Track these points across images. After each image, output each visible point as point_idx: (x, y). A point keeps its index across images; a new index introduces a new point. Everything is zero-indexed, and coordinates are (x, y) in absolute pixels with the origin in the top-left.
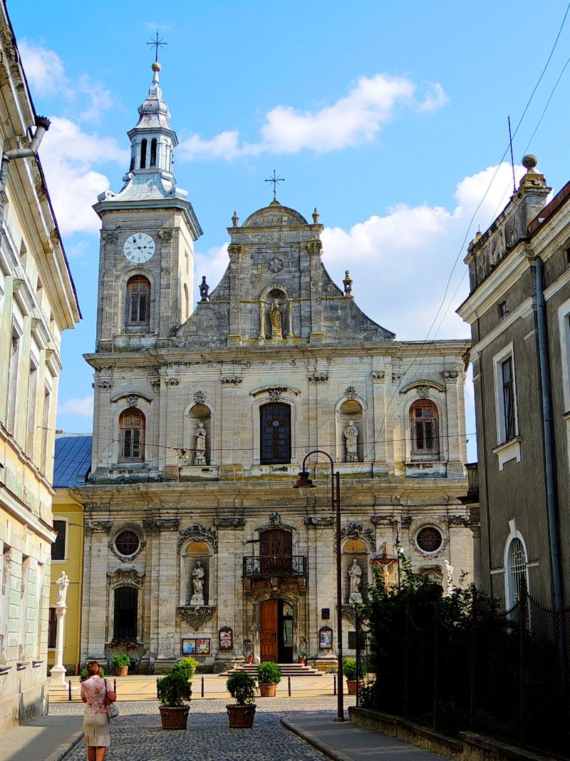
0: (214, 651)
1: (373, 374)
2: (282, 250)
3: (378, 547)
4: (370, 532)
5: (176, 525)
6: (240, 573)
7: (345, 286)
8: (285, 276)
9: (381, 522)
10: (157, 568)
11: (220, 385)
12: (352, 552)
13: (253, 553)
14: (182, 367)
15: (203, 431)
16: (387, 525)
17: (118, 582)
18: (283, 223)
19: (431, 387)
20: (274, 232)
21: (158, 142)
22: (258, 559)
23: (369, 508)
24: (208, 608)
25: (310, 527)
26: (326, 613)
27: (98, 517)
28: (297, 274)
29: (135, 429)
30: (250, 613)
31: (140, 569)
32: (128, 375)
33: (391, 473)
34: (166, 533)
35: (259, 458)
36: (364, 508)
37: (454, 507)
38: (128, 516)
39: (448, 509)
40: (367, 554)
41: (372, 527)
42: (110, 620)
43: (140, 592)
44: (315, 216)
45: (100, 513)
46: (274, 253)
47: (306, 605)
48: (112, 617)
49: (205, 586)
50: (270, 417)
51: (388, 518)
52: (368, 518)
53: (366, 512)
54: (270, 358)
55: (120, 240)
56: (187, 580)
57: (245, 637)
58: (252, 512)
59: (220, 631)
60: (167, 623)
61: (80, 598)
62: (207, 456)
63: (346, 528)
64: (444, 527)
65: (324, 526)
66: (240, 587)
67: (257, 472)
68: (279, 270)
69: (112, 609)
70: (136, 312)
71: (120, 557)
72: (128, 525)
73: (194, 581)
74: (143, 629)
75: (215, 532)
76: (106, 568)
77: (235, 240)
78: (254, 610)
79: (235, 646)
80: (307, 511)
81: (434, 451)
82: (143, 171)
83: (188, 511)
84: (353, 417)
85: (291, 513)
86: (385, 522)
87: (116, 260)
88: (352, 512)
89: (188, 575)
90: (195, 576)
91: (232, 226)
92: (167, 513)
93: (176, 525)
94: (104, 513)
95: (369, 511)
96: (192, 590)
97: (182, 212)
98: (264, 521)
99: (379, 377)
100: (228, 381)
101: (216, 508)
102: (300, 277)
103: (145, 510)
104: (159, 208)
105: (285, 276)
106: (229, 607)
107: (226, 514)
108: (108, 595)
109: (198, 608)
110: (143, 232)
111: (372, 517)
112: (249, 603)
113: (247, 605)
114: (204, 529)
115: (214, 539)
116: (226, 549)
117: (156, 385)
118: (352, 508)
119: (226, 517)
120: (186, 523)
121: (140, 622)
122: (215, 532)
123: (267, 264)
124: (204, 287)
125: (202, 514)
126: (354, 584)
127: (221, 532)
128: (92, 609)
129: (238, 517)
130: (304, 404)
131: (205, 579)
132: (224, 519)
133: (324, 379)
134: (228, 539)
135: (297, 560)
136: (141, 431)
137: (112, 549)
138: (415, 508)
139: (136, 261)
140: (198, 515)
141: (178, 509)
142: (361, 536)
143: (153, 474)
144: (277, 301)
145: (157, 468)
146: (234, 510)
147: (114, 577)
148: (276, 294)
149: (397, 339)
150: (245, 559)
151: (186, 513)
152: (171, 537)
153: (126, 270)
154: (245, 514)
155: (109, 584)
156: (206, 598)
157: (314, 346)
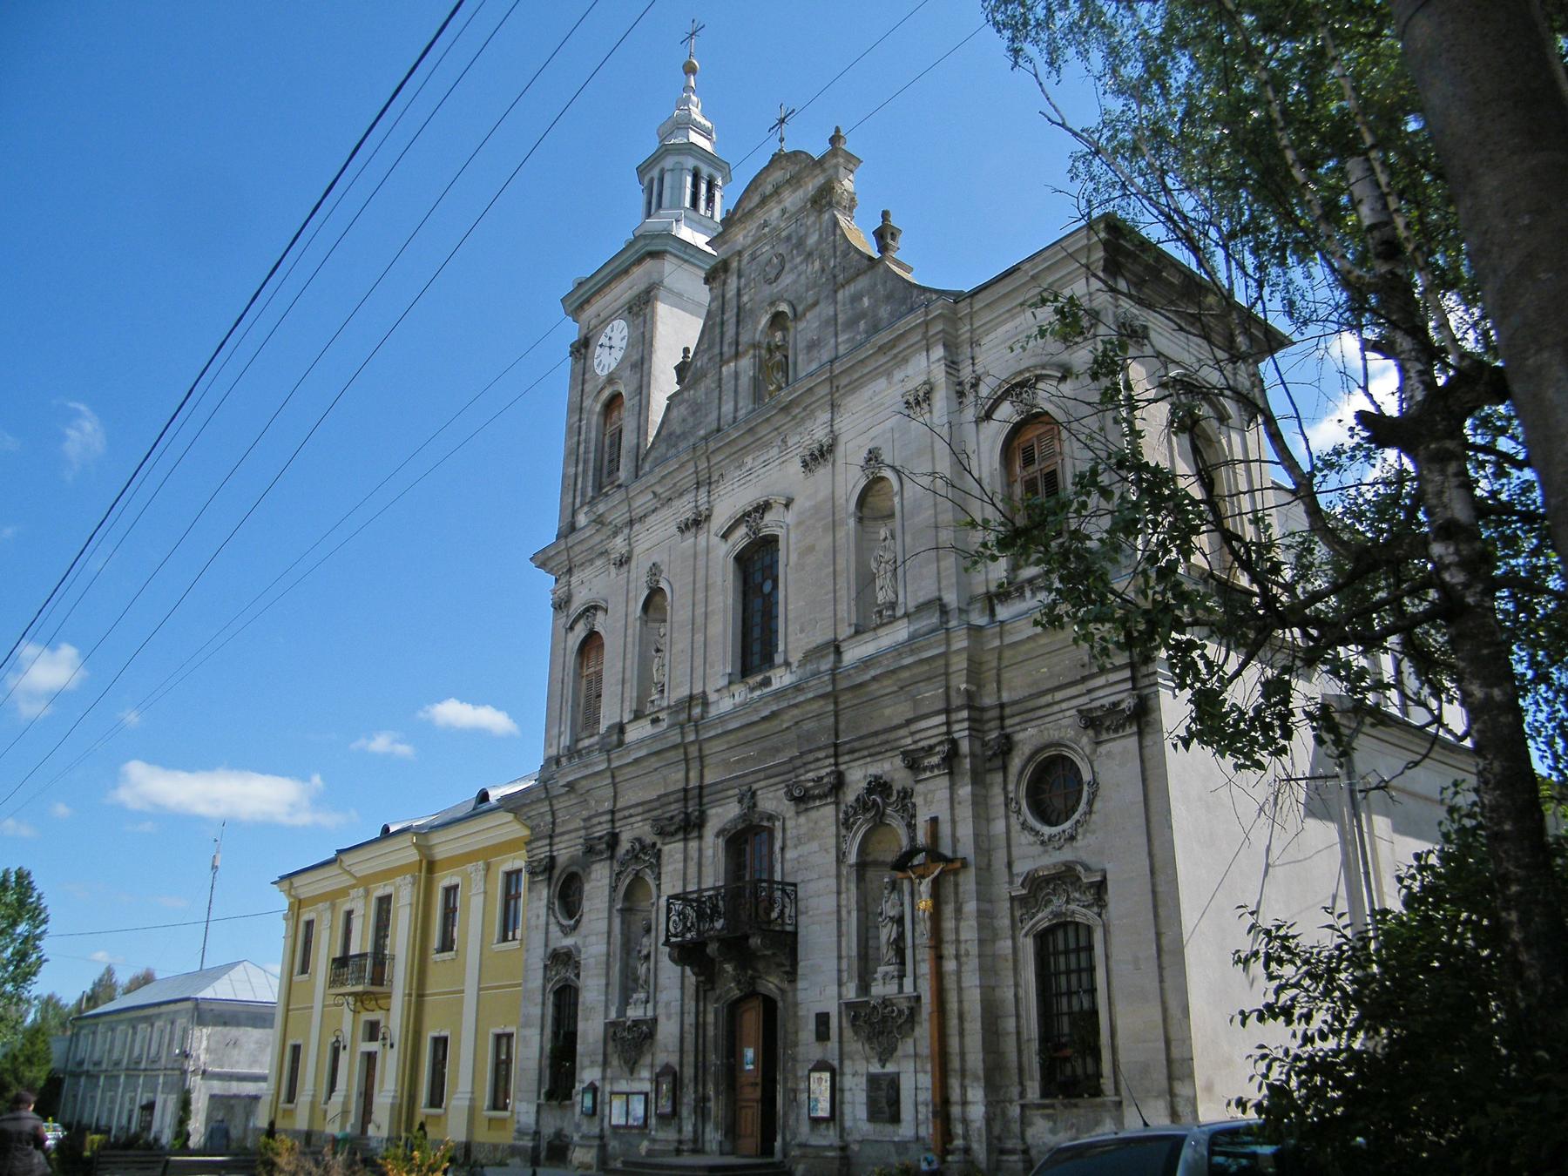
2: (784, 234)
14: (636, 527)
19: (1039, 378)
25: (802, 806)
36: (893, 736)
38: (573, 843)
47: (796, 1005)
48: (548, 1047)
52: (898, 762)
57: (700, 1089)
59: (658, 1076)
67: (724, 705)
71: (561, 926)
79: (685, 1112)
83: (626, 813)
85: (772, 781)
86: (935, 760)
88: (872, 751)
92: (600, 823)
95: (903, 742)
97: (668, 257)
99: (918, 403)
101: (659, 797)
105: (787, 279)
107: (673, 807)
108: (544, 1004)
109: (629, 1023)
118: (870, 742)
125: (646, 816)
130: (799, 524)
131: (647, 957)
138: (1016, 709)
139: (606, 372)
140: (639, 818)
144: (779, 335)
148: (778, 320)
151: (625, 818)
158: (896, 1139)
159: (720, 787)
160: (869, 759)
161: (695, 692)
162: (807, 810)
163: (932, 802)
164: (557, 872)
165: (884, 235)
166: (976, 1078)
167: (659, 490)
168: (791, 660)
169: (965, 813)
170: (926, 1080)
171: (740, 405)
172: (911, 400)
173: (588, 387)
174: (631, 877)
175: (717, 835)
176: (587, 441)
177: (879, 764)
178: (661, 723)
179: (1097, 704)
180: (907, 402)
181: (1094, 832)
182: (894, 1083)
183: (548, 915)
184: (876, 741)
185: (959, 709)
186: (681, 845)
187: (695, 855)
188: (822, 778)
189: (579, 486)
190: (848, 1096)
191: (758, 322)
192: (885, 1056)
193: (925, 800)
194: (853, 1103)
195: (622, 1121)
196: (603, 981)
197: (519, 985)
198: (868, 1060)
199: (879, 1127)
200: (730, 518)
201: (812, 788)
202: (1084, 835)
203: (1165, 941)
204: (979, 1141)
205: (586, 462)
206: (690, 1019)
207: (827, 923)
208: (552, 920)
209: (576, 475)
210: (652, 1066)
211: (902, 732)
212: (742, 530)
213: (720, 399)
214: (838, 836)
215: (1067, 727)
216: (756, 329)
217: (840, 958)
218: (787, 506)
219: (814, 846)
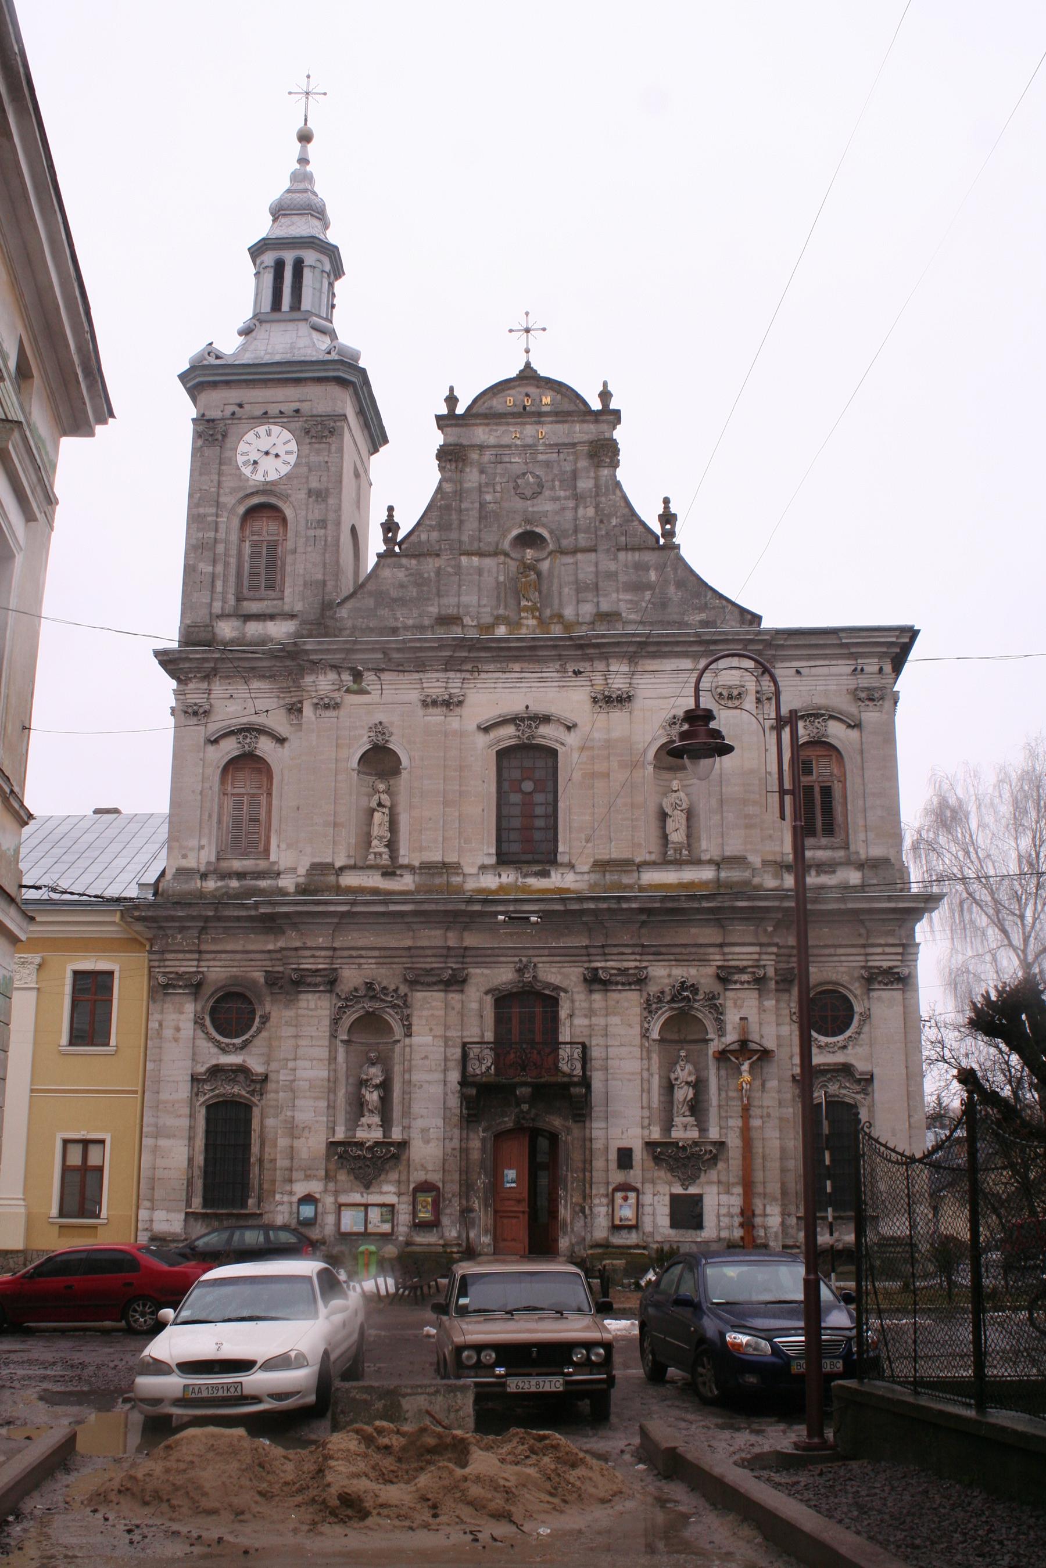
0: (402, 1230)
1: (719, 690)
2: (541, 457)
3: (729, 1027)
4: (713, 998)
5: (331, 981)
6: (454, 1076)
7: (663, 528)
8: (545, 506)
9: (736, 977)
10: (291, 1064)
11: (420, 711)
12: (675, 1037)
13: (483, 1036)
15: (385, 798)
16: (748, 982)
17: (212, 1090)
18: (545, 409)
19: (831, 717)
20: (525, 424)
21: (306, 263)
22: (491, 1049)
23: (711, 950)
24: (391, 1144)
25: (596, 987)
26: (625, 1158)
27: (177, 963)
28: (571, 504)
29: (253, 795)
30: (475, 1156)
31: (257, 1067)
32: (239, 689)
33: (756, 881)
34: (310, 996)
35: (493, 851)
36: (702, 950)
37: (879, 950)
38: (236, 964)
39: (867, 955)
40: (706, 1041)
41: (717, 988)
42: (196, 1163)
43: (256, 1112)
44: (605, 395)
45: (180, 956)
46: (526, 463)
47: (586, 1141)
48: (200, 1159)
49: (385, 1101)
50: (516, 774)
51: (750, 970)
52: (711, 970)
53: (707, 957)
54: (517, 659)
55: (229, 443)
56: (350, 1089)
57: (464, 1202)
58: (486, 957)
59: (416, 1190)
60: (309, 1172)
61: (138, 1121)
62: (392, 845)
63: (667, 989)
64: (857, 988)
65: (623, 984)
66: (454, 1102)
67: (490, 882)
68: (536, 495)
69: (200, 1142)
70: (258, 574)
72: (235, 980)
73: (363, 1091)
74: (260, 1185)
75: (406, 995)
76: (189, 1063)
77: (451, 440)
78: (483, 1150)
79: (445, 1221)
80: (589, 955)
81: (837, 841)
82: (276, 316)
83: (354, 953)
84: (679, 775)
86: (745, 977)
87: (220, 474)
89: (351, 1081)
90: (367, 1080)
91: (444, 411)
93: (331, 981)
94: (188, 956)
95: (712, 957)
96: (358, 1107)
97: (351, 389)
98: (504, 975)
99: (730, 697)
100: (434, 703)
101: (409, 948)
102: (576, 509)
103: (269, 952)
104: (306, 379)
105: (545, 506)
106: (433, 1144)
107: (429, 960)
108: (192, 1116)
110: (275, 423)
111: (718, 967)
112: (472, 1135)
113: (467, 1139)
114: (385, 988)
115: (403, 1005)
116: (427, 1028)
117: (295, 710)
119: (428, 966)
120: (351, 977)
121: (255, 1170)
122: (406, 995)
123: (512, 485)
124: (390, 526)
125: (379, 960)
126: (681, 1100)
127: (419, 996)
128: (162, 1142)
129: (454, 966)
130: (582, 749)
131: (385, 1086)
132: (425, 969)
133: (623, 700)
134: (432, 1008)
135: (568, 1050)
136: (263, 799)
137: (203, 1025)
139: (259, 477)
140: (373, 961)
141: (335, 949)
142: (696, 1005)
143: (287, 883)
144: (529, 553)
145: (294, 870)
146: (445, 952)
147: (205, 1081)
148: (529, 539)
149: (765, 624)
150: (464, 1045)
151: (351, 957)
152: (319, 1003)
153: (241, 494)
154: (468, 960)
155: (197, 1095)
156: (386, 1123)
157: (603, 636)
158: (699, 1240)
159: (490, 952)
160: (674, 963)
161: (447, 860)
162: (607, 990)
163: (741, 1007)
164: (207, 990)
165: (668, 518)
166: (775, 1199)
167: (395, 655)
168: (573, 861)
169: (770, 1017)
170: (735, 1201)
171: (484, 602)
172: (725, 693)
173: (228, 483)
174: (362, 1012)
175: (487, 993)
176: (226, 542)
177: (685, 969)
178: (398, 878)
179: (870, 964)
180: (721, 694)
181: (861, 1046)
182: (698, 1199)
183: (195, 1030)
184: (683, 950)
185: (769, 945)
186: (442, 995)
187: (458, 1006)
188: (628, 969)
189: (219, 587)
190: (648, 1209)
191: (510, 532)
192: (691, 1179)
193: (735, 1004)
194: (654, 1214)
195: (362, 1229)
196: (323, 1104)
197: (136, 1092)
198: (670, 1184)
199: (682, 1232)
200: (500, 716)
201: (615, 975)
202: (853, 1047)
203: (912, 1120)
204: (776, 1240)
205: (226, 565)
206: (456, 1143)
207: (630, 1080)
208: (200, 1034)
209: (213, 577)
210: (399, 1182)
211: (717, 950)
212: (510, 730)
213: (460, 586)
214: (641, 1015)
215: (843, 973)
216: (504, 536)
217: (642, 1108)
218: (569, 728)
219: (614, 1020)
